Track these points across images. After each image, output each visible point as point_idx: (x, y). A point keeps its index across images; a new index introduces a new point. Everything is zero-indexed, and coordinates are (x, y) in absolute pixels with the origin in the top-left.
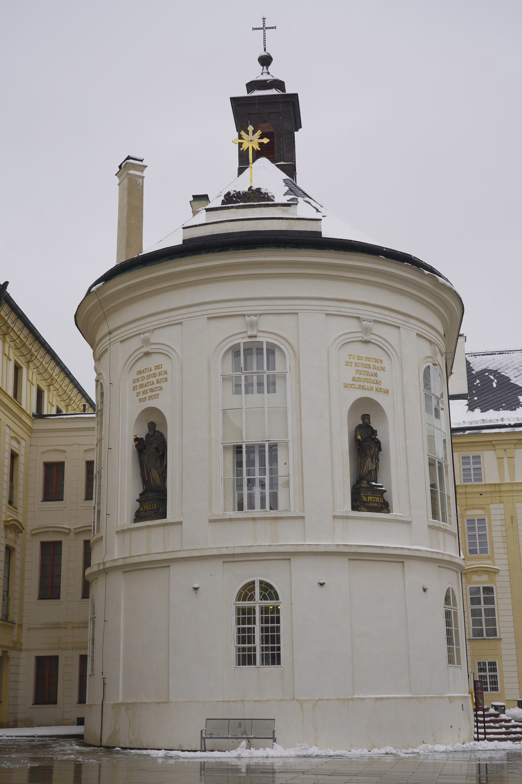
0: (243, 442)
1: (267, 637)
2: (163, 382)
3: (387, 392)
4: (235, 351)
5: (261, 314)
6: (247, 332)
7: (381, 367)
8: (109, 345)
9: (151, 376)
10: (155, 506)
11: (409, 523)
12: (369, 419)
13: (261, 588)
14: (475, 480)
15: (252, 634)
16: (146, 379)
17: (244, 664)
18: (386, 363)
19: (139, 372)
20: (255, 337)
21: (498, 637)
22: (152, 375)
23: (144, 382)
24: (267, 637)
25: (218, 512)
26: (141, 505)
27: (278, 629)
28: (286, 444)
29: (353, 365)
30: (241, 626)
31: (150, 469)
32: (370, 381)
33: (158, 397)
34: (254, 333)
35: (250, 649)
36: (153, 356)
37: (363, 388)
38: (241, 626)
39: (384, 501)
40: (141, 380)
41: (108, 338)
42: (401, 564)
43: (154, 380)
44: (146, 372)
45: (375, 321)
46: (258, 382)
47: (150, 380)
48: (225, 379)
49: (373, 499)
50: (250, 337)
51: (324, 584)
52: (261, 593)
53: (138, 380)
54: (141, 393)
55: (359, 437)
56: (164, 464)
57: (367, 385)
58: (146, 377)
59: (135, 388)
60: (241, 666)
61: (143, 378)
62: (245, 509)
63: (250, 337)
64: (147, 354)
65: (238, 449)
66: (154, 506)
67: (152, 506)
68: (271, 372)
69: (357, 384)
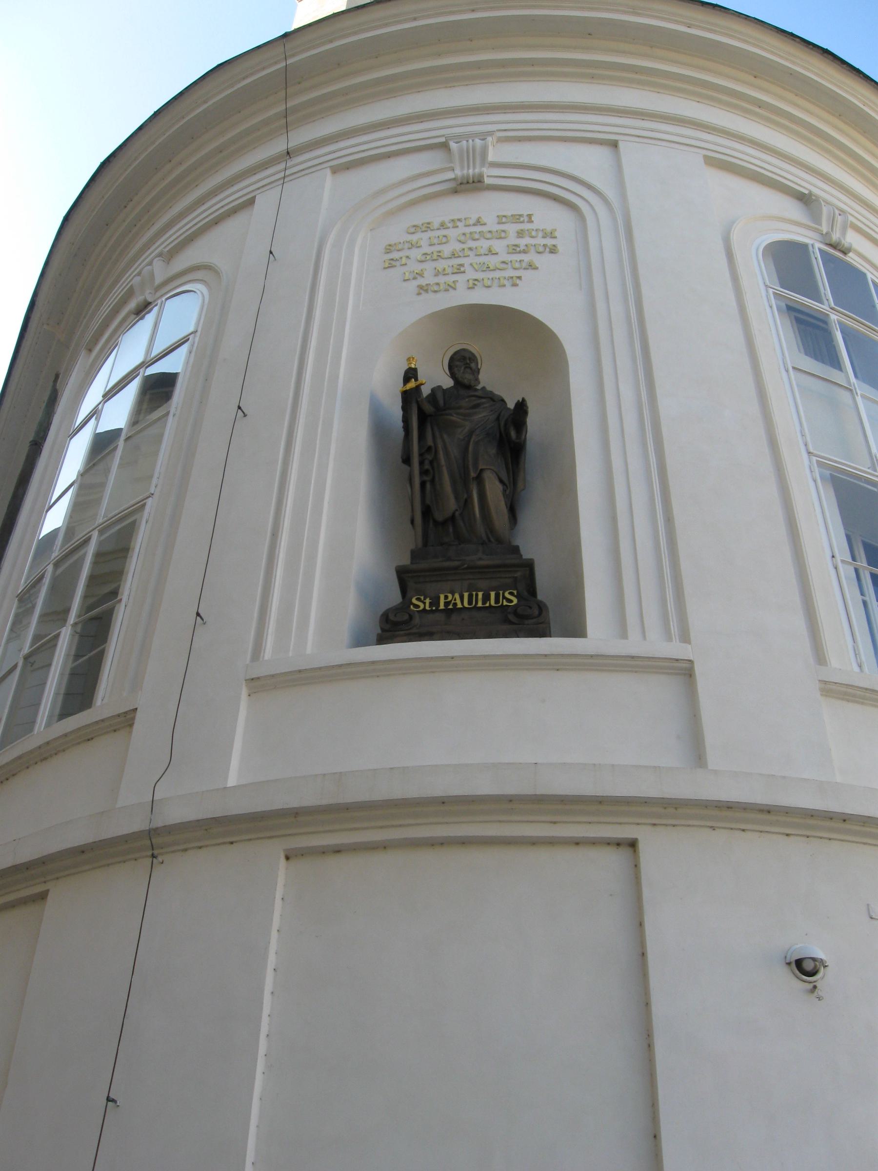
10: (507, 595)
31: (482, 470)
43: (499, 246)
66: (504, 597)
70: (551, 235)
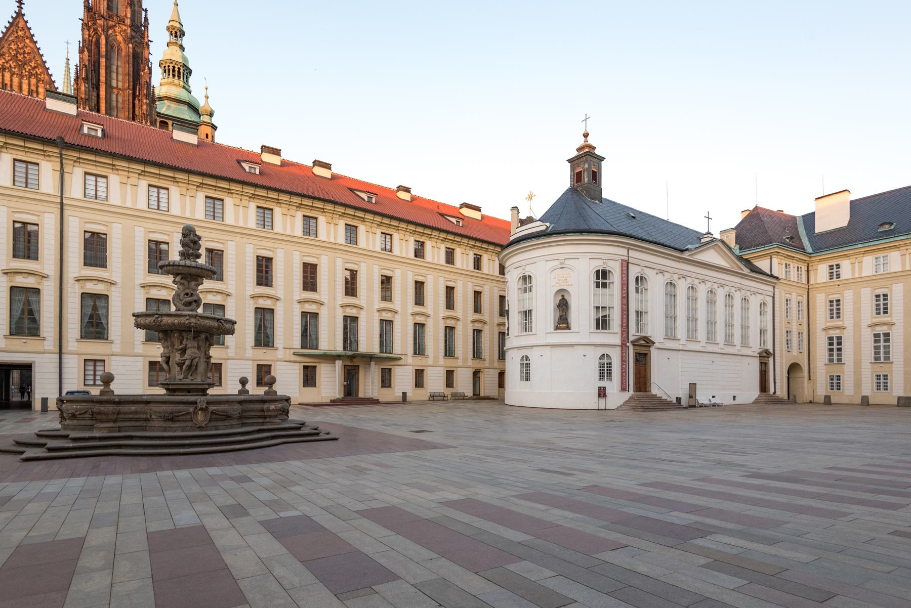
3: (572, 285)
11: (579, 332)
14: (837, 278)
21: (843, 362)
25: (517, 334)
45: (565, 259)
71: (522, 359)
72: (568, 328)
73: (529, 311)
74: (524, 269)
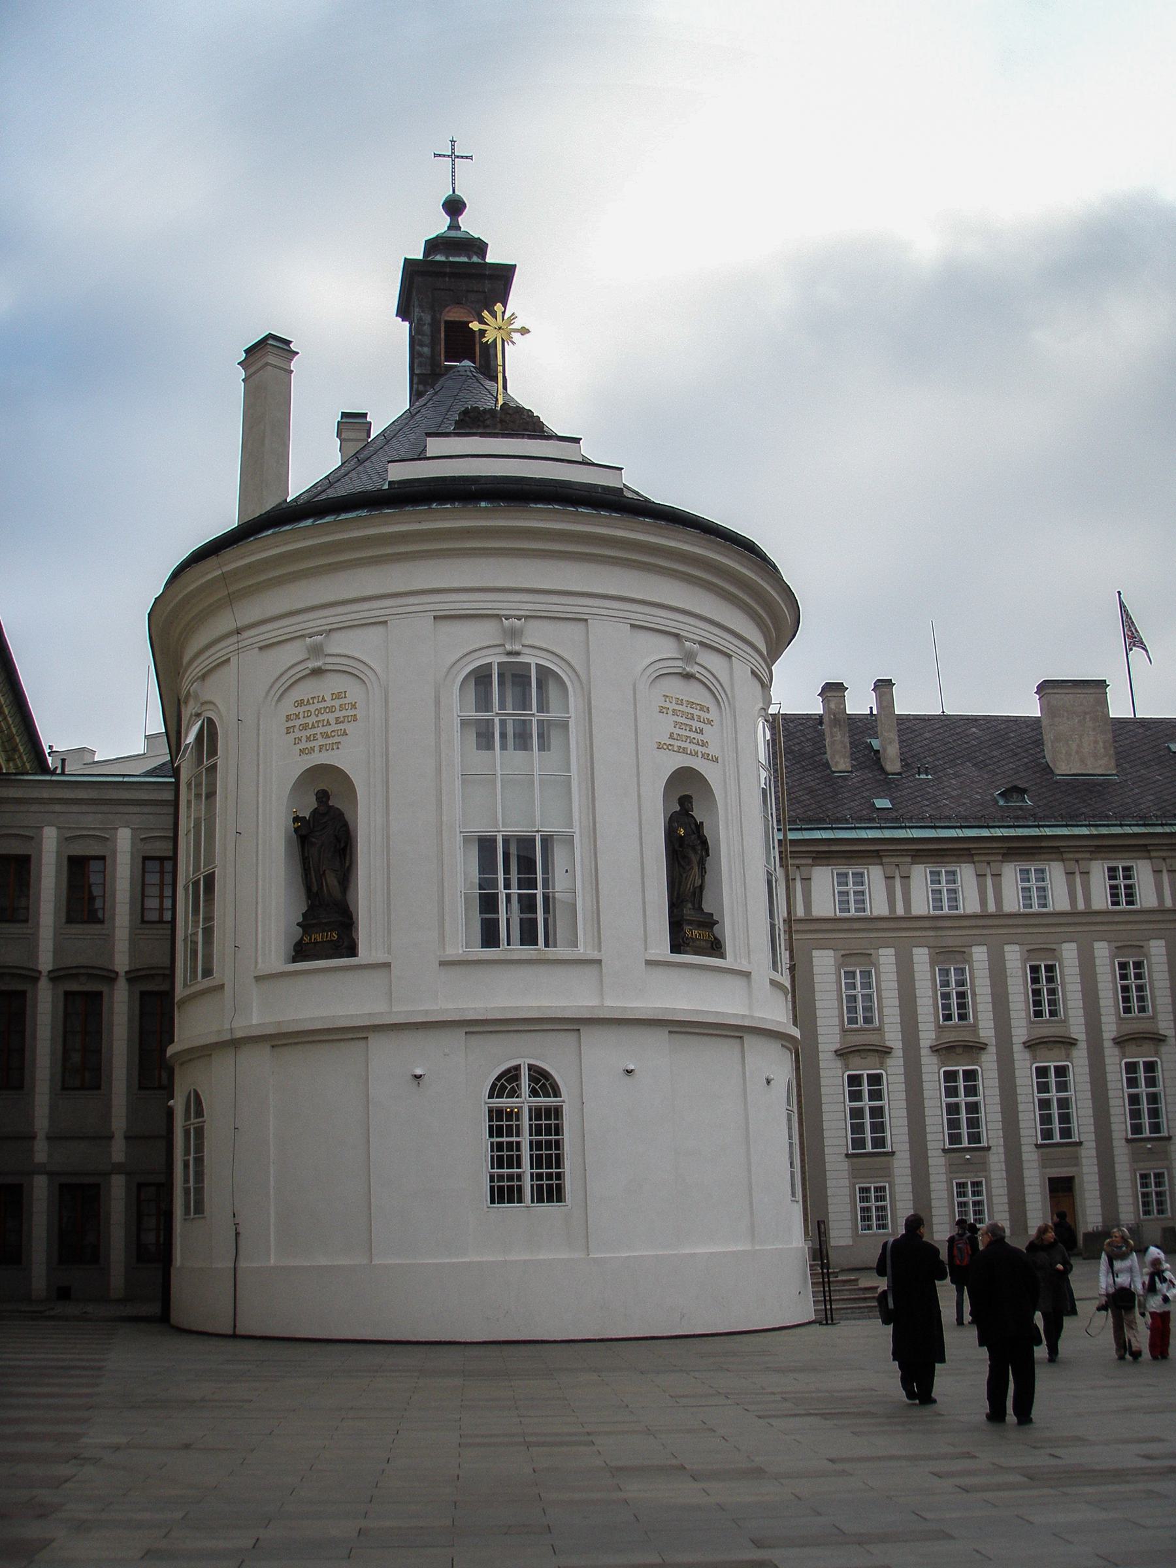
0: (499, 831)
1: (539, 1157)
2: (349, 722)
3: (716, 760)
4: (481, 677)
5: (527, 617)
6: (504, 645)
7: (708, 719)
8: (237, 652)
9: (325, 710)
12: (691, 803)
13: (531, 1078)
15: (515, 1153)
16: (313, 716)
17: (501, 1201)
18: (713, 715)
19: (300, 703)
20: (518, 654)
22: (325, 708)
23: (313, 719)
24: (539, 1157)
26: (305, 932)
27: (558, 1145)
28: (570, 840)
29: (670, 712)
30: (496, 1140)
32: (694, 741)
33: (338, 748)
34: (517, 648)
35: (510, 1177)
36: (329, 675)
37: (684, 751)
38: (496, 1140)
39: (716, 939)
40: (304, 717)
41: (234, 639)
42: (738, 1040)
43: (332, 717)
44: (314, 703)
45: (702, 644)
46: (517, 731)
47: (321, 717)
48: (465, 723)
49: (700, 935)
50: (510, 653)
51: (632, 1071)
52: (529, 1085)
53: (297, 716)
54: (304, 739)
55: (682, 831)
56: (347, 865)
57: (690, 747)
58: (313, 711)
59: (292, 730)
60: (496, 1205)
61: (308, 714)
62: (503, 944)
63: (510, 653)
64: (317, 672)
65: (486, 845)
67: (327, 934)
68: (543, 716)
69: (677, 743)
70: (354, 706)
71: (506, 1083)
72: (715, 948)
73: (506, 840)
74: (514, 634)
